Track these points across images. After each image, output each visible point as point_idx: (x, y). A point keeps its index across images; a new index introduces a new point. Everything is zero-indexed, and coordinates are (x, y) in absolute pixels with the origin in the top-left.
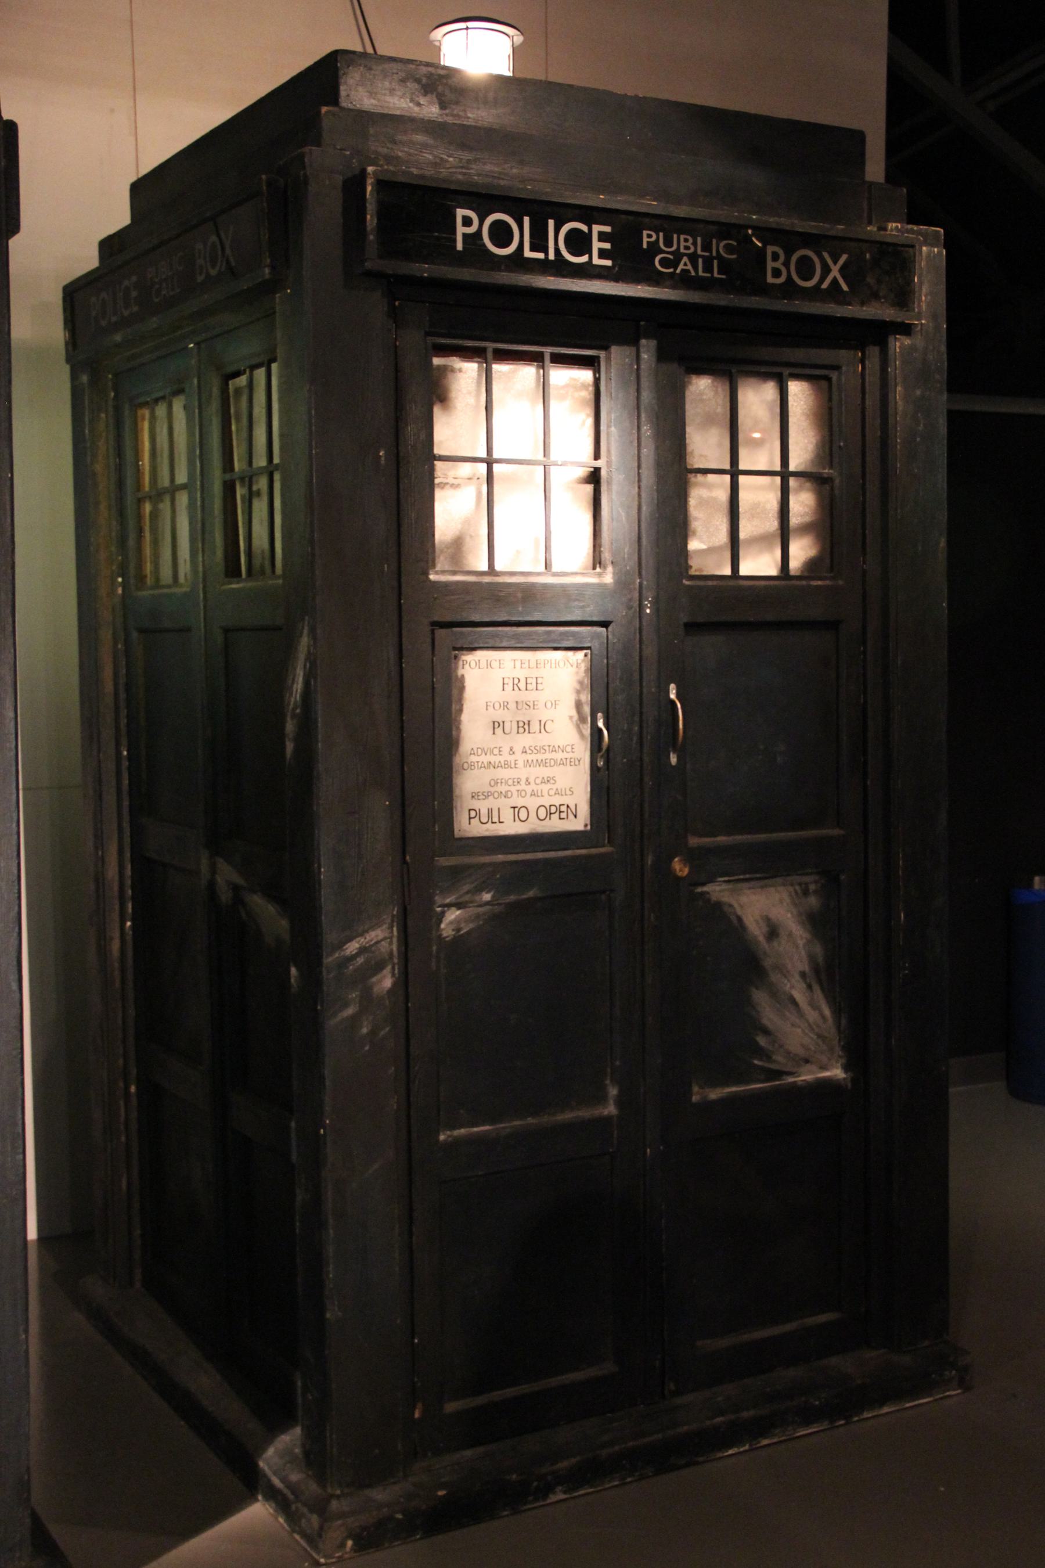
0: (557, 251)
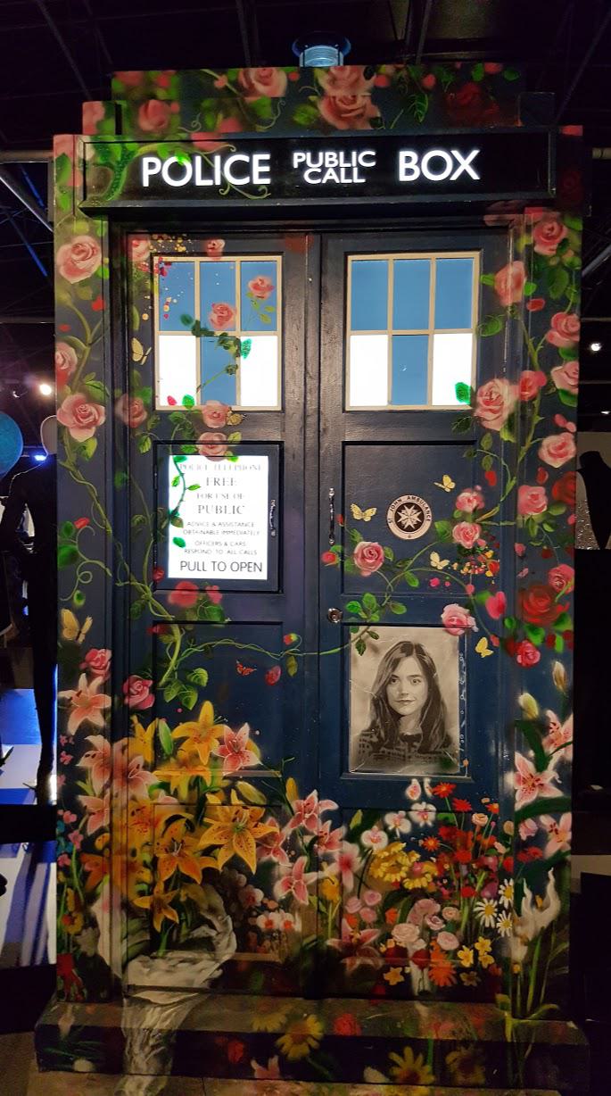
0: (223, 178)
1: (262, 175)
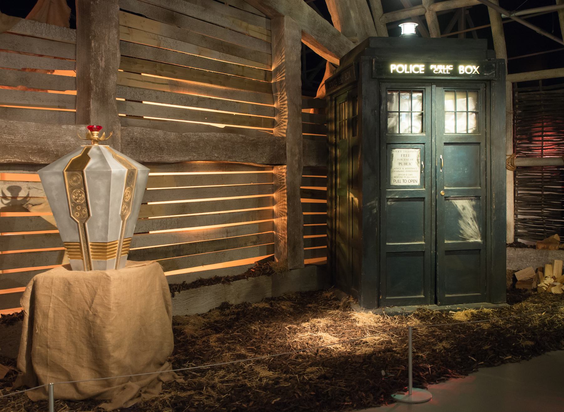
1: (422, 71)
